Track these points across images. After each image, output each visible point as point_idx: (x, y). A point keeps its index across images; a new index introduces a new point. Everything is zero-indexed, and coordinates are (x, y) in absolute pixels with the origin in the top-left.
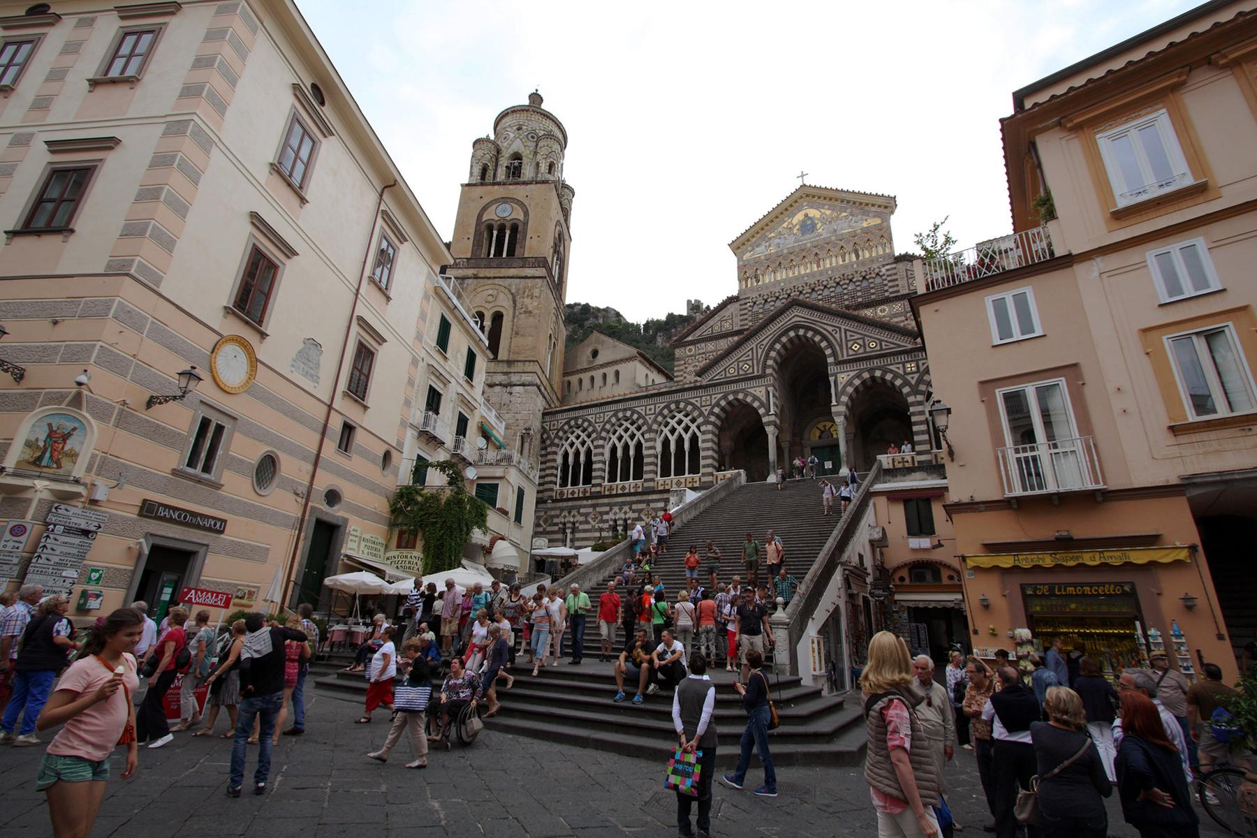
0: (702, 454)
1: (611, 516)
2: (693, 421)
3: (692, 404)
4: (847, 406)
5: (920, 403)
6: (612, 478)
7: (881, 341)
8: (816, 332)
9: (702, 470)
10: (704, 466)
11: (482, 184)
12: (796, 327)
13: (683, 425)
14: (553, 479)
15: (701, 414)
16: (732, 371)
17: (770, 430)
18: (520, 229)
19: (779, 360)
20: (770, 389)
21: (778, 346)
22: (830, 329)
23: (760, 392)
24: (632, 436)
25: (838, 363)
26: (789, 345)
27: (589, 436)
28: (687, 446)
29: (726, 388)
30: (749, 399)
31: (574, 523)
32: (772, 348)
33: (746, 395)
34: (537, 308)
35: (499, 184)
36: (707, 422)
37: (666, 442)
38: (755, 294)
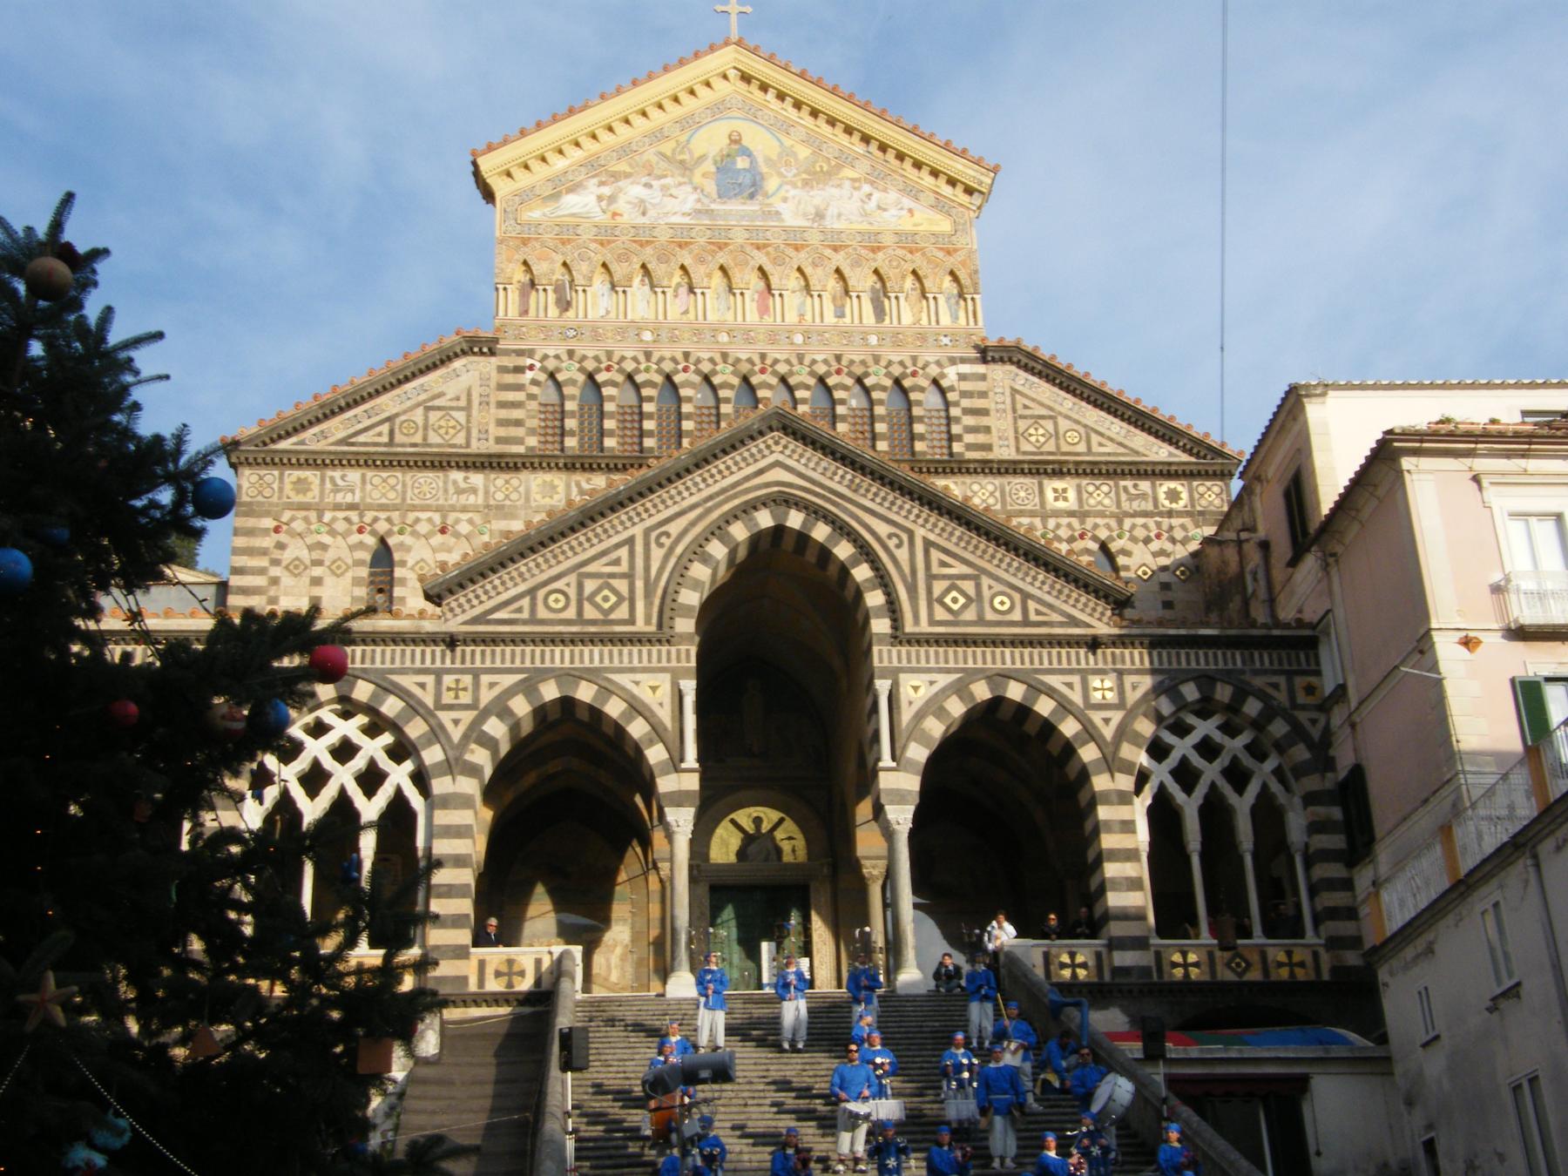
2: (399, 752)
3: (402, 693)
5: (1124, 799)
7: (1026, 596)
8: (842, 530)
12: (783, 501)
15: (437, 734)
16: (557, 601)
20: (689, 687)
21: (718, 550)
22: (883, 529)
25: (898, 637)
29: (529, 656)
30: (614, 708)
32: (697, 552)
33: (607, 691)
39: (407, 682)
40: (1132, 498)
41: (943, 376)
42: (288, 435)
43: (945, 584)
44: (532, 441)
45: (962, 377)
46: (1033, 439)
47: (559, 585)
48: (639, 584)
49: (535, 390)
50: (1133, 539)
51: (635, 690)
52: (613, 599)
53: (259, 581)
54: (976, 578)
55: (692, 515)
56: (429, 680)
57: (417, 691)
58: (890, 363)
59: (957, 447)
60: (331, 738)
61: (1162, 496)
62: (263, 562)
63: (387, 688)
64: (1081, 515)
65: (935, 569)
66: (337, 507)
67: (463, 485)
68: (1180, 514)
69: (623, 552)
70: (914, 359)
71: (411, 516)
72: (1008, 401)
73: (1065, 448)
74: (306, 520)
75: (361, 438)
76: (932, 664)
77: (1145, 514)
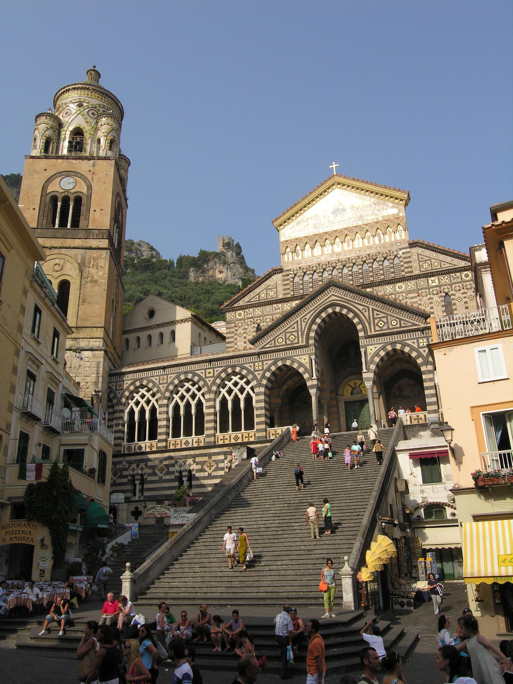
0: (256, 412)
1: (177, 468)
2: (248, 383)
4: (375, 373)
6: (176, 434)
7: (401, 320)
9: (256, 427)
10: (258, 423)
11: (46, 157)
12: (333, 305)
13: (239, 386)
14: (120, 435)
16: (280, 340)
17: (313, 392)
18: (84, 201)
19: (319, 332)
20: (313, 357)
21: (318, 321)
22: (361, 308)
23: (305, 360)
24: (194, 396)
25: (367, 337)
26: (327, 320)
27: (153, 395)
28: (242, 405)
29: (274, 356)
30: (295, 366)
31: (142, 475)
32: (313, 322)
34: (102, 277)
35: (62, 157)
36: (259, 385)
37: (224, 402)
38: (295, 267)
39: (247, 366)
40: (454, 279)
41: (398, 254)
43: (379, 320)
44: (292, 293)
45: (403, 253)
46: (424, 267)
48: (300, 333)
49: (292, 280)
50: (456, 291)
52: (294, 338)
53: (232, 340)
54: (387, 317)
56: (252, 365)
57: (249, 368)
58: (383, 253)
59: (403, 273)
60: (232, 381)
61: (463, 276)
62: (233, 335)
63: (243, 368)
64: (440, 286)
65: (375, 316)
66: (248, 318)
67: (276, 308)
68: (469, 281)
69: (296, 325)
70: (390, 251)
71: (265, 318)
72: (417, 258)
73: (434, 268)
74: (241, 323)
75: (252, 300)
76: (376, 342)
77: (458, 283)
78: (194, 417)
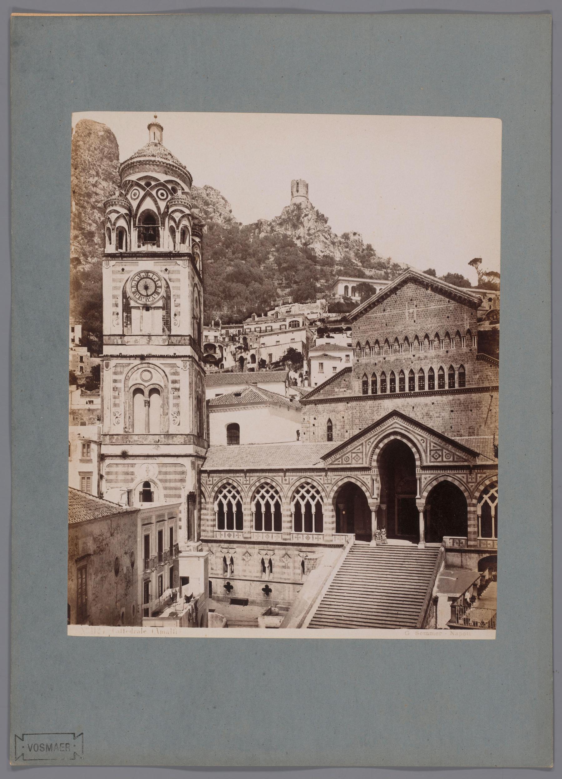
5: (474, 505)
32: (376, 446)
36: (328, 496)
42: (310, 397)
47: (347, 455)
48: (364, 453)
51: (363, 480)
55: (376, 437)
78: (273, 515)
